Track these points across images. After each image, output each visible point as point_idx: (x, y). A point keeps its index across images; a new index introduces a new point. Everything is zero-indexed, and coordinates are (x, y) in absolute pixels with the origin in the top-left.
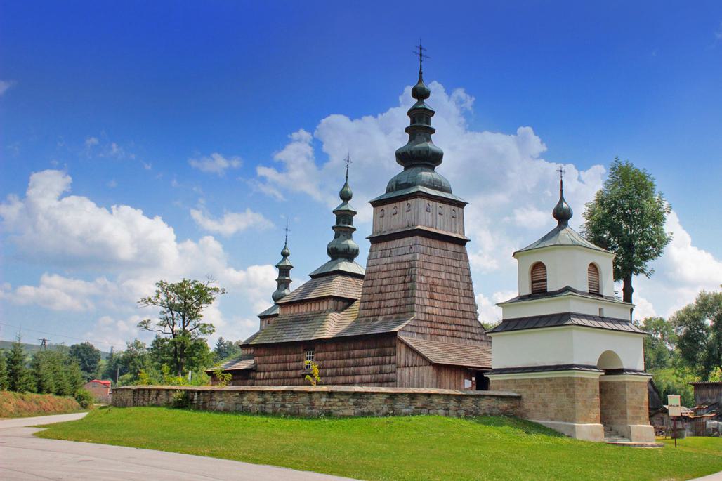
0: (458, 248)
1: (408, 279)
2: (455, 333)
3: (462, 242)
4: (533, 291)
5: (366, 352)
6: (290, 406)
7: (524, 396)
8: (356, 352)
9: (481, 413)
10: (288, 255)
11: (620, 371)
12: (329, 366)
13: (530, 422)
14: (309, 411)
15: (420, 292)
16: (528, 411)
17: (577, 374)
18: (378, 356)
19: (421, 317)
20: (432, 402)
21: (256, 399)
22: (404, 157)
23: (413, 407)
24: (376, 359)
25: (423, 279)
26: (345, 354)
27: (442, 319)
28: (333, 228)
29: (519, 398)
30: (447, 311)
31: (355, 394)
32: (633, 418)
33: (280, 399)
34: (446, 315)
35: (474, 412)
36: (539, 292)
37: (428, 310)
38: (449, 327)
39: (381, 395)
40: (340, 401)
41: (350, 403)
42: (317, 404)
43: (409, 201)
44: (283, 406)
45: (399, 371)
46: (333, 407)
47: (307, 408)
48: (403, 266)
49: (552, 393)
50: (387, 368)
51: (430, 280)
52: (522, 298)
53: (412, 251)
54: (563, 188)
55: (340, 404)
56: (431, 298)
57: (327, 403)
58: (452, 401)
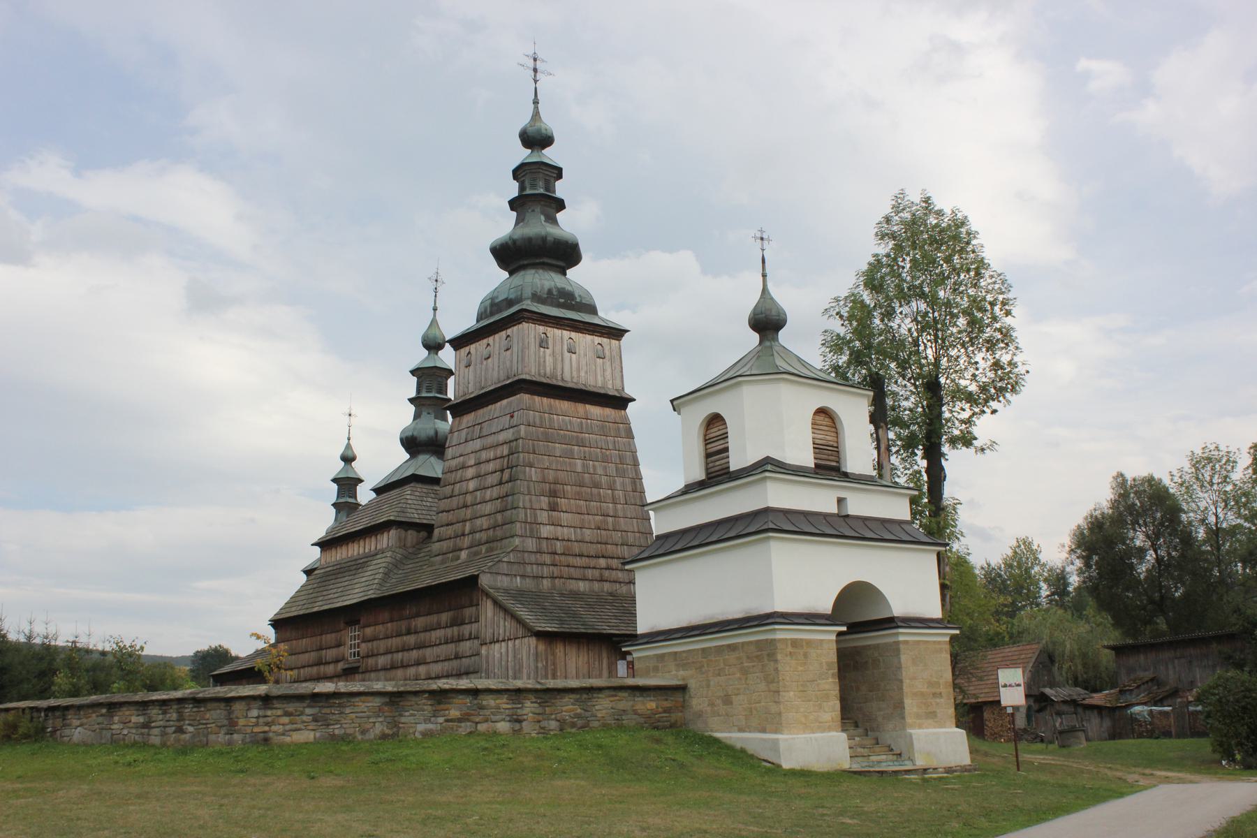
0: (609, 412)
1: (506, 476)
2: (606, 574)
3: (621, 402)
4: (707, 474)
5: (433, 619)
6: (191, 729)
7: (692, 684)
8: (420, 622)
9: (596, 724)
10: (354, 459)
11: (890, 623)
12: (382, 651)
13: (717, 740)
14: (227, 737)
15: (527, 498)
16: (700, 715)
17: (783, 633)
18: (452, 626)
19: (531, 544)
20: (482, 708)
21: (134, 719)
22: (509, 255)
23: (441, 720)
24: (449, 632)
25: (533, 474)
26: (403, 625)
27: (576, 548)
28: (411, 400)
29: (683, 689)
30: (588, 532)
31: (315, 697)
32: (918, 716)
33: (175, 716)
34: (587, 539)
35: (580, 723)
36: (717, 474)
37: (546, 531)
38: (593, 562)
39: (370, 698)
40: (287, 714)
41: (305, 718)
42: (242, 722)
43: (509, 331)
44: (180, 730)
45: (484, 651)
46: (274, 728)
47: (223, 731)
48: (499, 452)
49: (738, 675)
50: (466, 647)
51: (551, 475)
52: (689, 489)
53: (515, 421)
54: (767, 271)
55: (286, 720)
56: (553, 508)
57: (261, 720)
58: (528, 704)
